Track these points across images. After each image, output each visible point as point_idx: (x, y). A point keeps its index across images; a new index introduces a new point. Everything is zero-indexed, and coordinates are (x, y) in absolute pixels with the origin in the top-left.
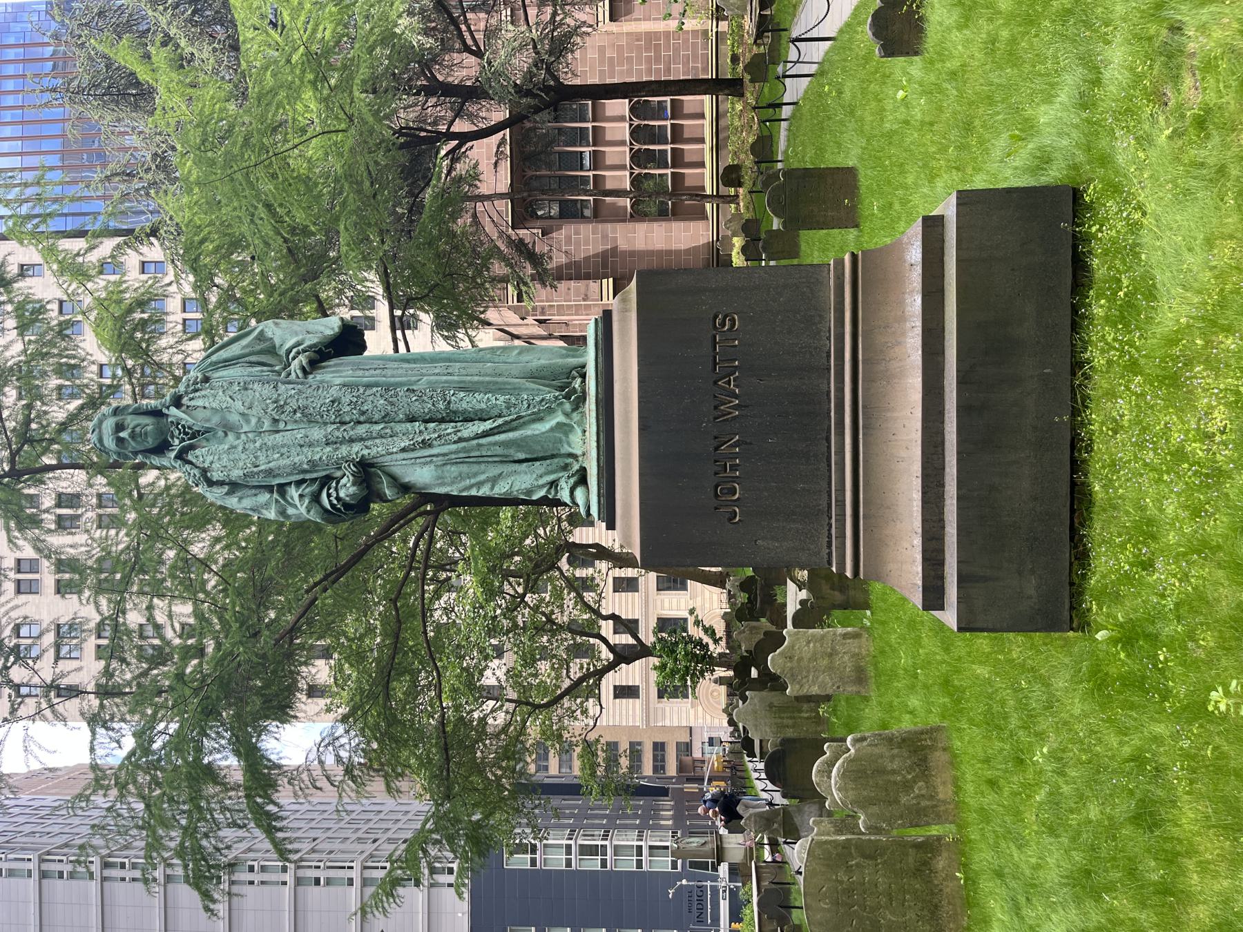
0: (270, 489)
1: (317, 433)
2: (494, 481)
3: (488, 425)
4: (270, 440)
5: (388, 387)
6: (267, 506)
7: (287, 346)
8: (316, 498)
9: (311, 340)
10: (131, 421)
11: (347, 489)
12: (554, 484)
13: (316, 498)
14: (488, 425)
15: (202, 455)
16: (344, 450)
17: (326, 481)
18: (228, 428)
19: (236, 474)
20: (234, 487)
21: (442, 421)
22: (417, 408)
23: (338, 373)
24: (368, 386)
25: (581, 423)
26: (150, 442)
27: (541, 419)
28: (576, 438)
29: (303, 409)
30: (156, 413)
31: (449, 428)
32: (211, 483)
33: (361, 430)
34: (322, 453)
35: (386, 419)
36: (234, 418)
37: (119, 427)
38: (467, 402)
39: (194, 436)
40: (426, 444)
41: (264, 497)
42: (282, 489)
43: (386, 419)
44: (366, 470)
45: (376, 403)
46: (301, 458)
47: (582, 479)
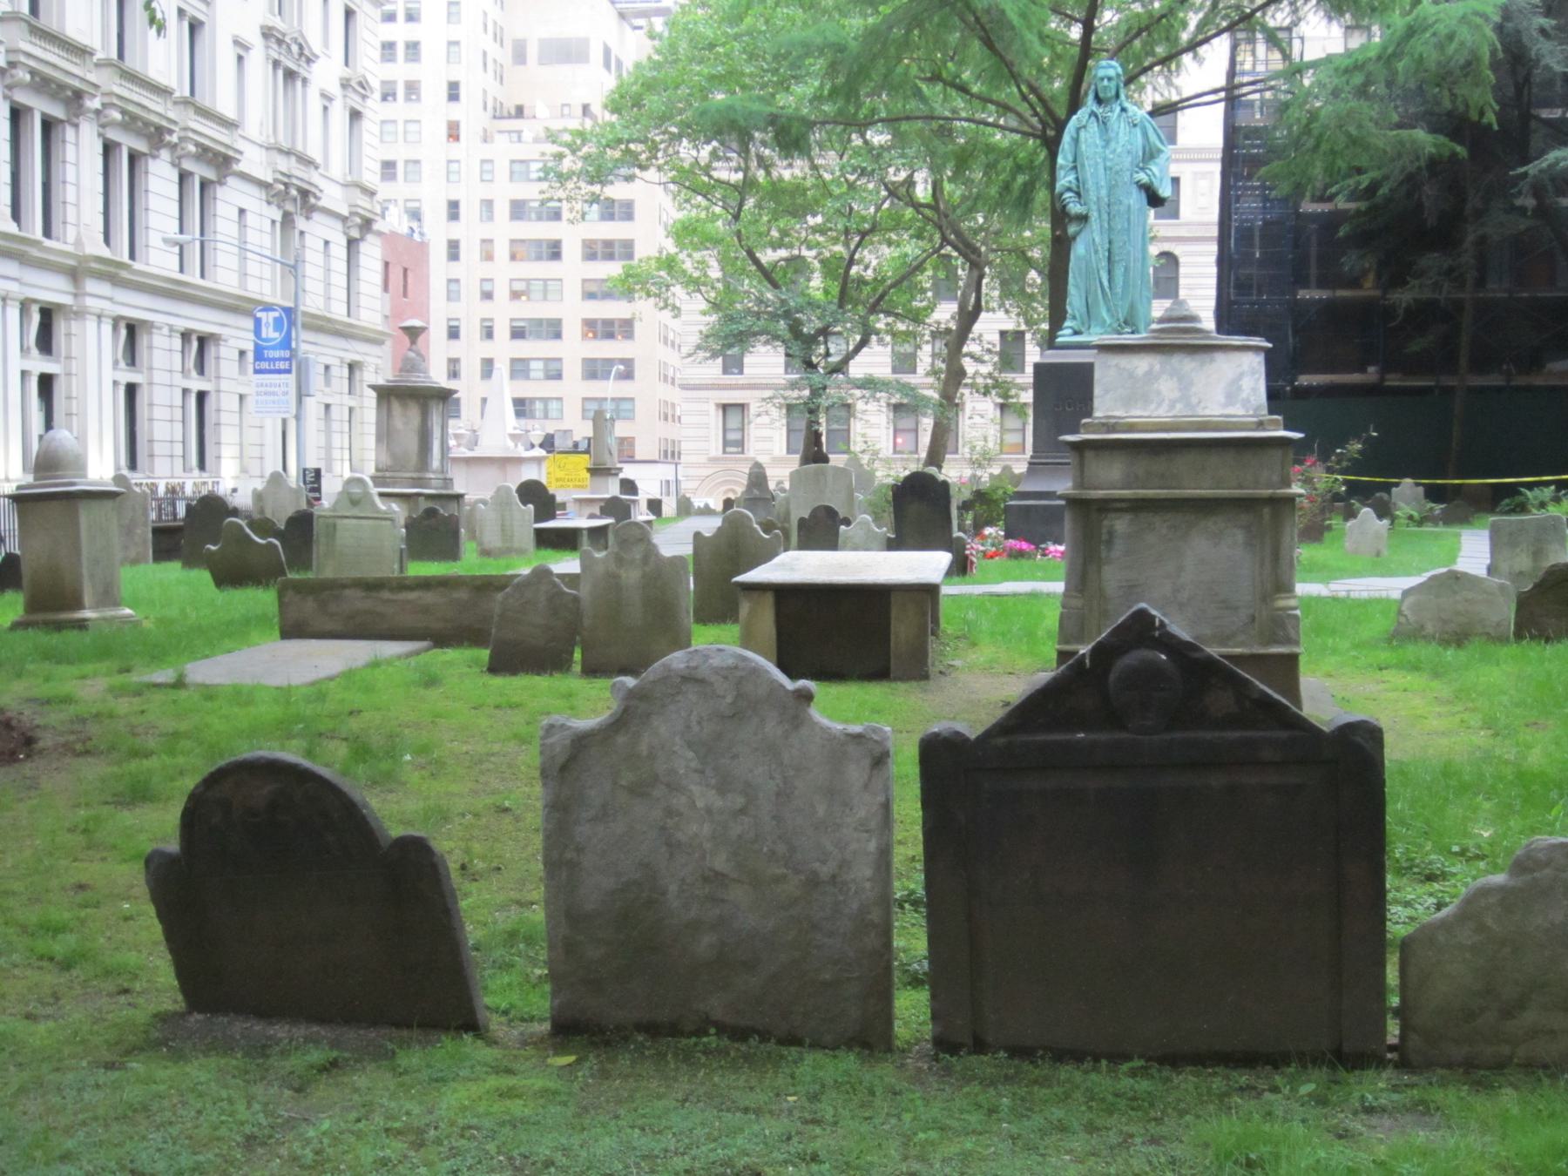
0: (1075, 161)
1: (1104, 192)
2: (1077, 286)
3: (1106, 283)
4: (1101, 167)
5: (1128, 230)
6: (1065, 158)
7: (1154, 169)
8: (1069, 189)
9: (1156, 183)
10: (1113, 84)
11: (1075, 208)
12: (1074, 318)
13: (1069, 189)
14: (1106, 283)
15: (1094, 127)
16: (1094, 207)
17: (1078, 194)
18: (1107, 142)
19: (1083, 147)
20: (1076, 141)
21: (1109, 258)
22: (1116, 245)
23: (1136, 199)
24: (1129, 220)
25: (1106, 333)
26: (1101, 95)
27: (1109, 310)
28: (1098, 330)
29: (1116, 185)
30: (1117, 96)
31: (1104, 263)
32: (1078, 130)
33: (1105, 216)
34: (1093, 196)
35: (1110, 229)
36: (1113, 145)
37: (1110, 79)
38: (1119, 272)
39: (1104, 123)
40: (1096, 252)
41: (1070, 158)
42: (1075, 168)
43: (1110, 229)
44: (1083, 219)
45: (1119, 224)
46: (1090, 184)
47: (1076, 333)
